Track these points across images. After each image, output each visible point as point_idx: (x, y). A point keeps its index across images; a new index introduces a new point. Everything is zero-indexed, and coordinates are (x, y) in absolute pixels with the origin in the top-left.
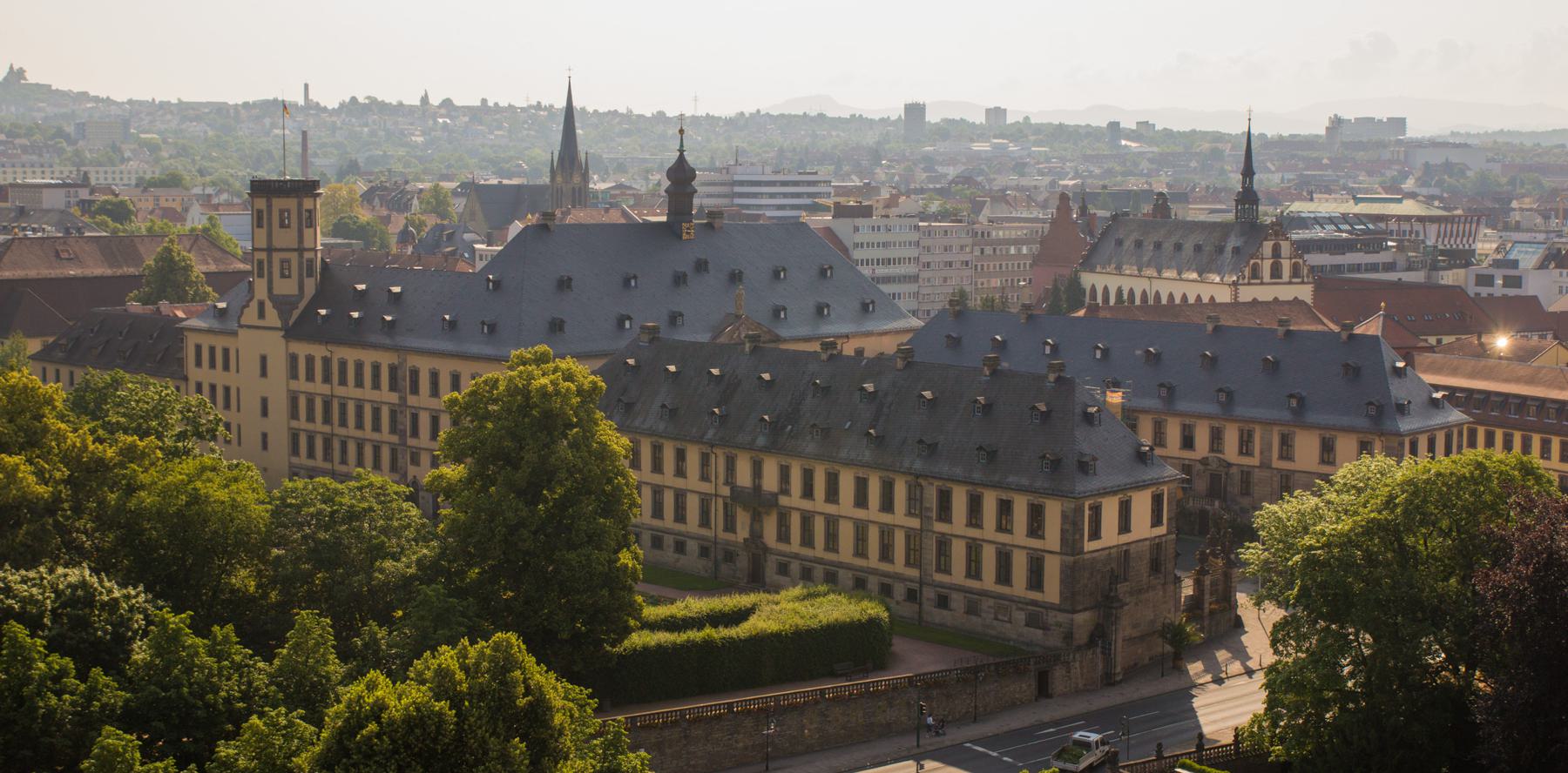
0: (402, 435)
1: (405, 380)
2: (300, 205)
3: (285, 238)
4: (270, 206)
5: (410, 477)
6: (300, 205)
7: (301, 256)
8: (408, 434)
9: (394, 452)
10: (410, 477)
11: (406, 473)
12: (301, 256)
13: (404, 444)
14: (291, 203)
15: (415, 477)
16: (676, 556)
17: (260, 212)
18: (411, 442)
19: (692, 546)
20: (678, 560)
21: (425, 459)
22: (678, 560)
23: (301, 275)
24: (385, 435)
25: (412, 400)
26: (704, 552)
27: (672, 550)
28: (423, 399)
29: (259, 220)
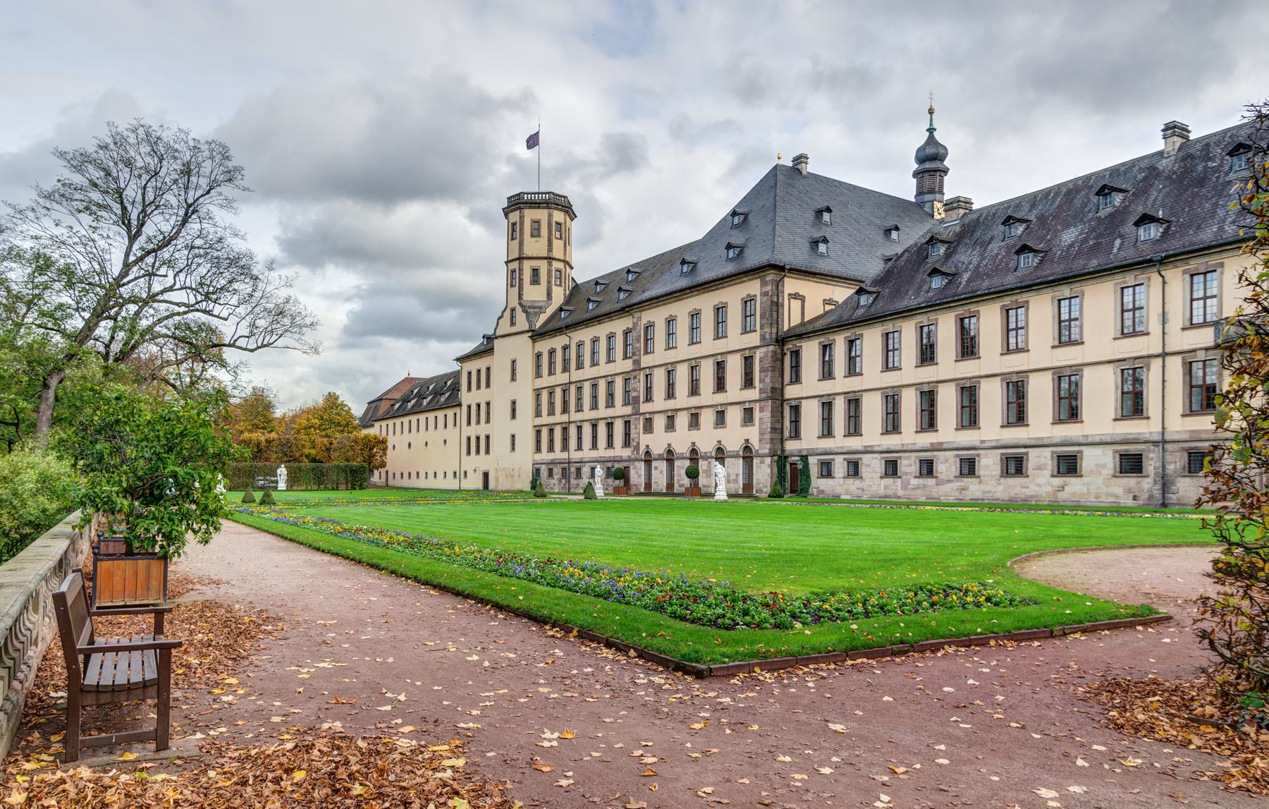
0: (636, 401)
1: (638, 341)
2: (550, 216)
3: (535, 247)
4: (522, 218)
5: (642, 448)
6: (550, 216)
7: (550, 264)
8: (641, 400)
9: (627, 424)
10: (642, 448)
11: (638, 443)
12: (550, 264)
13: (637, 413)
14: (542, 214)
15: (647, 446)
16: (1058, 481)
17: (514, 224)
18: (645, 407)
19: (1099, 462)
20: (1062, 488)
21: (659, 422)
22: (1062, 488)
23: (549, 282)
24: (620, 409)
25: (646, 361)
26: (1131, 464)
27: (1048, 473)
28: (660, 355)
29: (514, 232)
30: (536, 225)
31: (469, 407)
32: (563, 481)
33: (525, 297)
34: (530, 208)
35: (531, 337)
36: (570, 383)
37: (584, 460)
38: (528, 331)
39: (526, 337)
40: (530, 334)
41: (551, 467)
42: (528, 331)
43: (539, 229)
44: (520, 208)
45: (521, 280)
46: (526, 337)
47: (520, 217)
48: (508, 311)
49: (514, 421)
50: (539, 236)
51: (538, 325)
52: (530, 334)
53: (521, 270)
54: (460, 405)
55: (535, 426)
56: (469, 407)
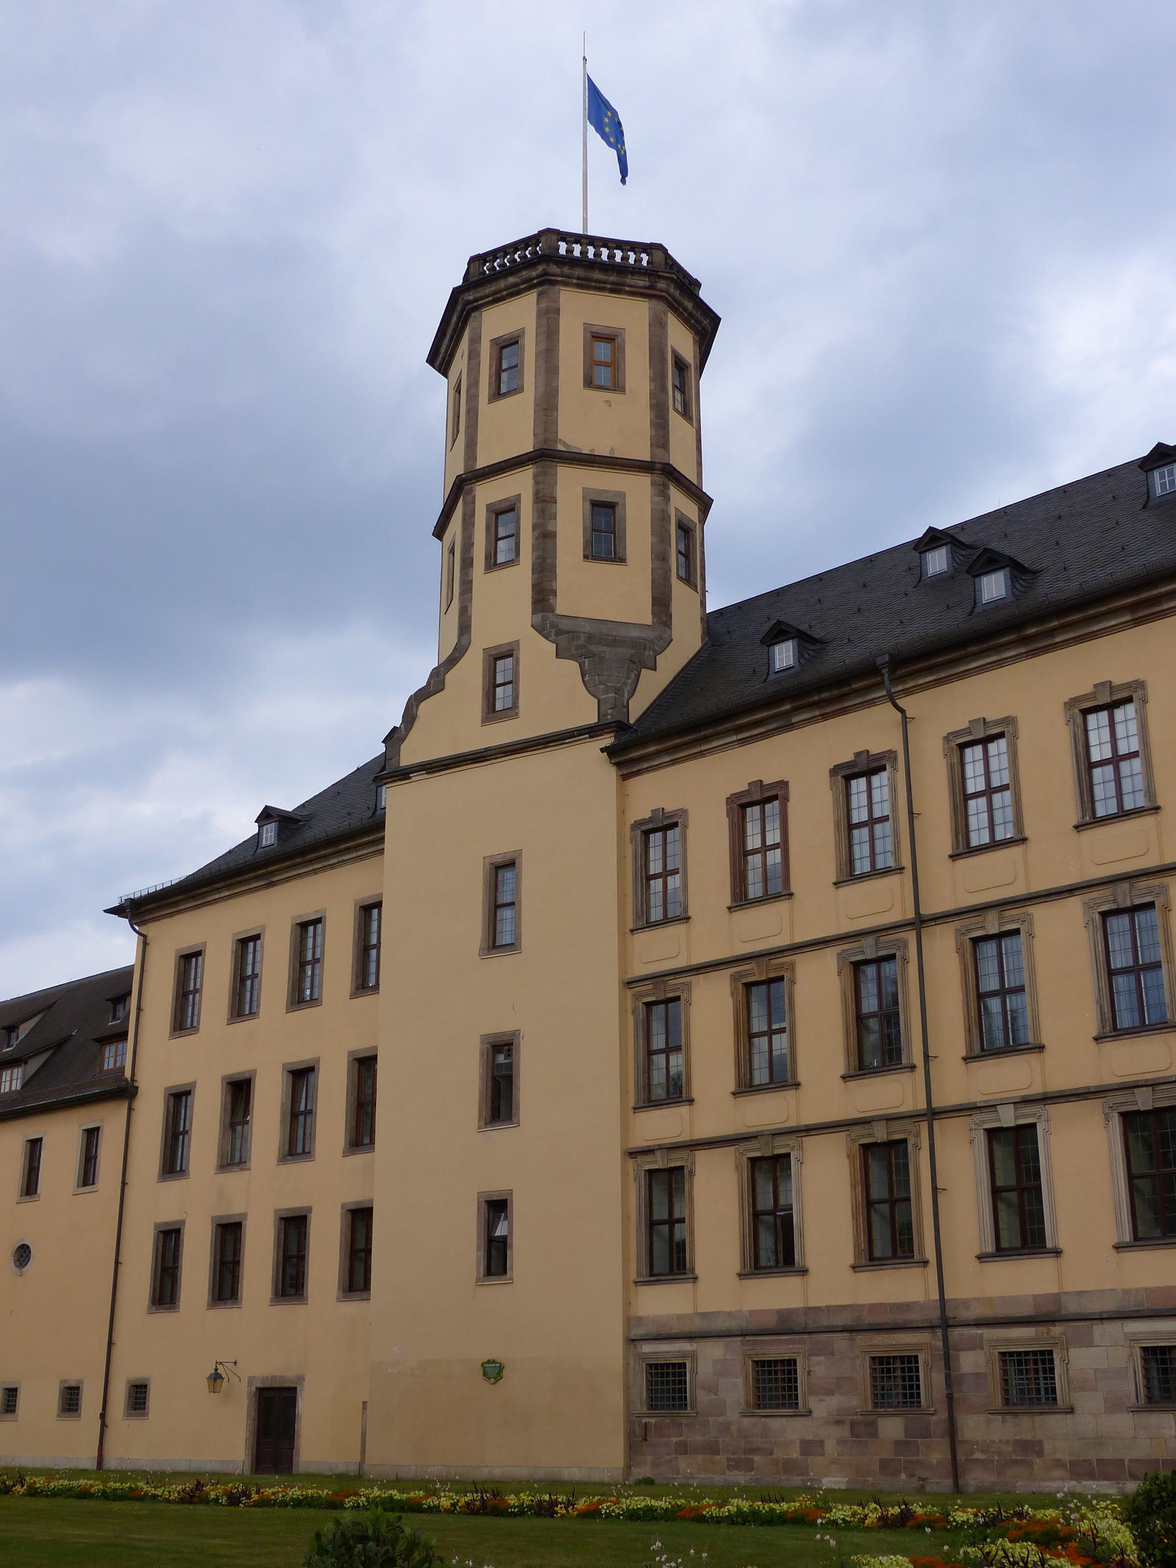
30: (603, 351)
31: (179, 1099)
32: (892, 1427)
33: (564, 604)
34: (584, 284)
35: (609, 751)
36: (920, 923)
37: (1071, 1307)
38: (592, 732)
39: (592, 751)
40: (607, 740)
41: (776, 1350)
42: (592, 732)
43: (616, 365)
44: (546, 281)
45: (545, 537)
46: (592, 751)
47: (541, 314)
48: (472, 666)
49: (501, 1135)
50: (617, 386)
51: (637, 707)
52: (607, 740)
53: (545, 501)
54: (125, 1092)
55: (633, 1154)
56: (179, 1099)
